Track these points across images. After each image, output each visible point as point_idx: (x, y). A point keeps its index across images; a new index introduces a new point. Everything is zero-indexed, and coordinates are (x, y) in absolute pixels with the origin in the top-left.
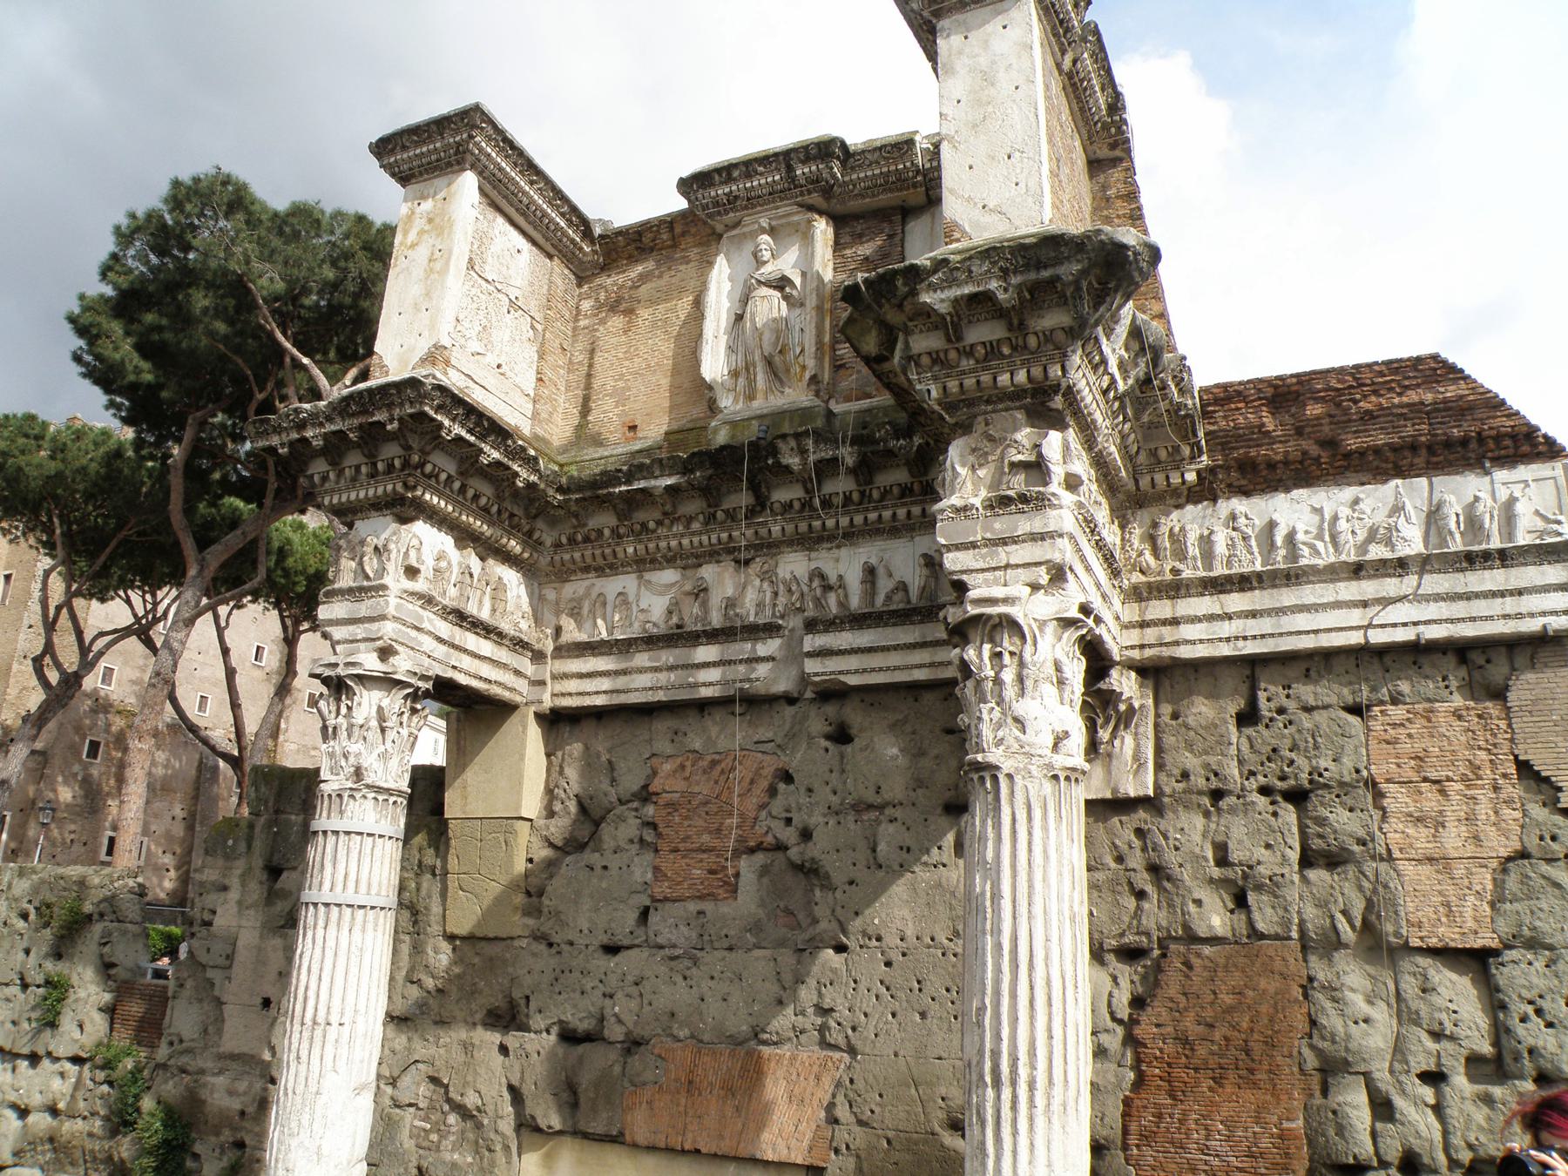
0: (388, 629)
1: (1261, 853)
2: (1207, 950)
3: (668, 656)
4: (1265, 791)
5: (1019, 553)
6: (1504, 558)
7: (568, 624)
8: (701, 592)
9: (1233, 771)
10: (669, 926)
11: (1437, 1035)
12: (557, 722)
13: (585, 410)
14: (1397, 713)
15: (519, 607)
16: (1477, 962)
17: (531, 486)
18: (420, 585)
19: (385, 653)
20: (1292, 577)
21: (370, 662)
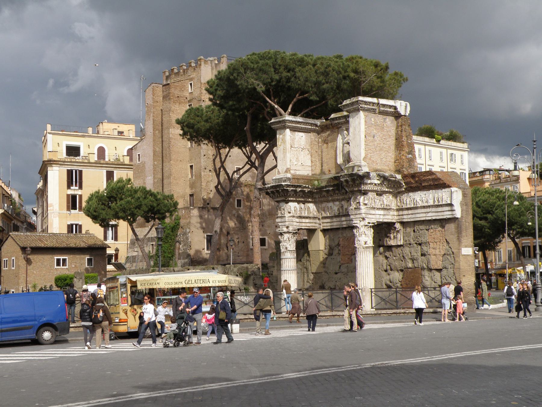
0: (287, 223)
1: (415, 254)
2: (410, 270)
3: (338, 219)
4: (416, 243)
5: (358, 216)
6: (441, 206)
7: (323, 213)
8: (342, 207)
9: (412, 241)
10: (343, 269)
11: (435, 282)
12: (324, 231)
13: (322, 166)
14: (432, 231)
15: (314, 210)
16: (439, 270)
17: (308, 191)
18: (291, 215)
19: (287, 227)
20: (416, 208)
21: (285, 230)
